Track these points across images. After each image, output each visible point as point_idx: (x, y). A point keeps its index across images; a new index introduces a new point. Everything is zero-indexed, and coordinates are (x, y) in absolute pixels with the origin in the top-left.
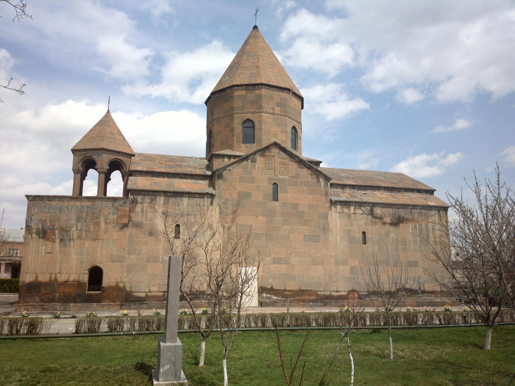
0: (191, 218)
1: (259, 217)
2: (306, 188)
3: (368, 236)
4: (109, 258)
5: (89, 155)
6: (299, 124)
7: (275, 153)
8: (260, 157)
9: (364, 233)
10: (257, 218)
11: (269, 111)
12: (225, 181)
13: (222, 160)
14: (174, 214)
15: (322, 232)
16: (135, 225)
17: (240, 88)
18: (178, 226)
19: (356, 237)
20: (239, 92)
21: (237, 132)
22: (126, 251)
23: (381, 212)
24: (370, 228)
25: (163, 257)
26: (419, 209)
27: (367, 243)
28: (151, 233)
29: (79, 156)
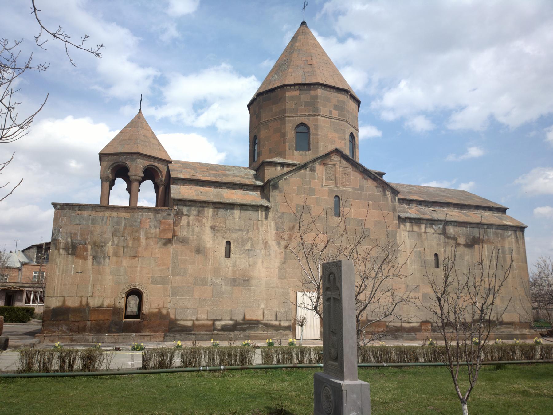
0: (243, 233)
3: (441, 258)
4: (150, 279)
5: (120, 160)
7: (337, 161)
9: (436, 255)
11: (326, 115)
12: (280, 192)
13: (274, 169)
14: (224, 229)
16: (181, 240)
17: (292, 87)
18: (228, 243)
19: (427, 259)
20: (291, 92)
22: (170, 272)
23: (454, 231)
25: (212, 279)
26: (495, 229)
28: (199, 251)
29: (108, 161)
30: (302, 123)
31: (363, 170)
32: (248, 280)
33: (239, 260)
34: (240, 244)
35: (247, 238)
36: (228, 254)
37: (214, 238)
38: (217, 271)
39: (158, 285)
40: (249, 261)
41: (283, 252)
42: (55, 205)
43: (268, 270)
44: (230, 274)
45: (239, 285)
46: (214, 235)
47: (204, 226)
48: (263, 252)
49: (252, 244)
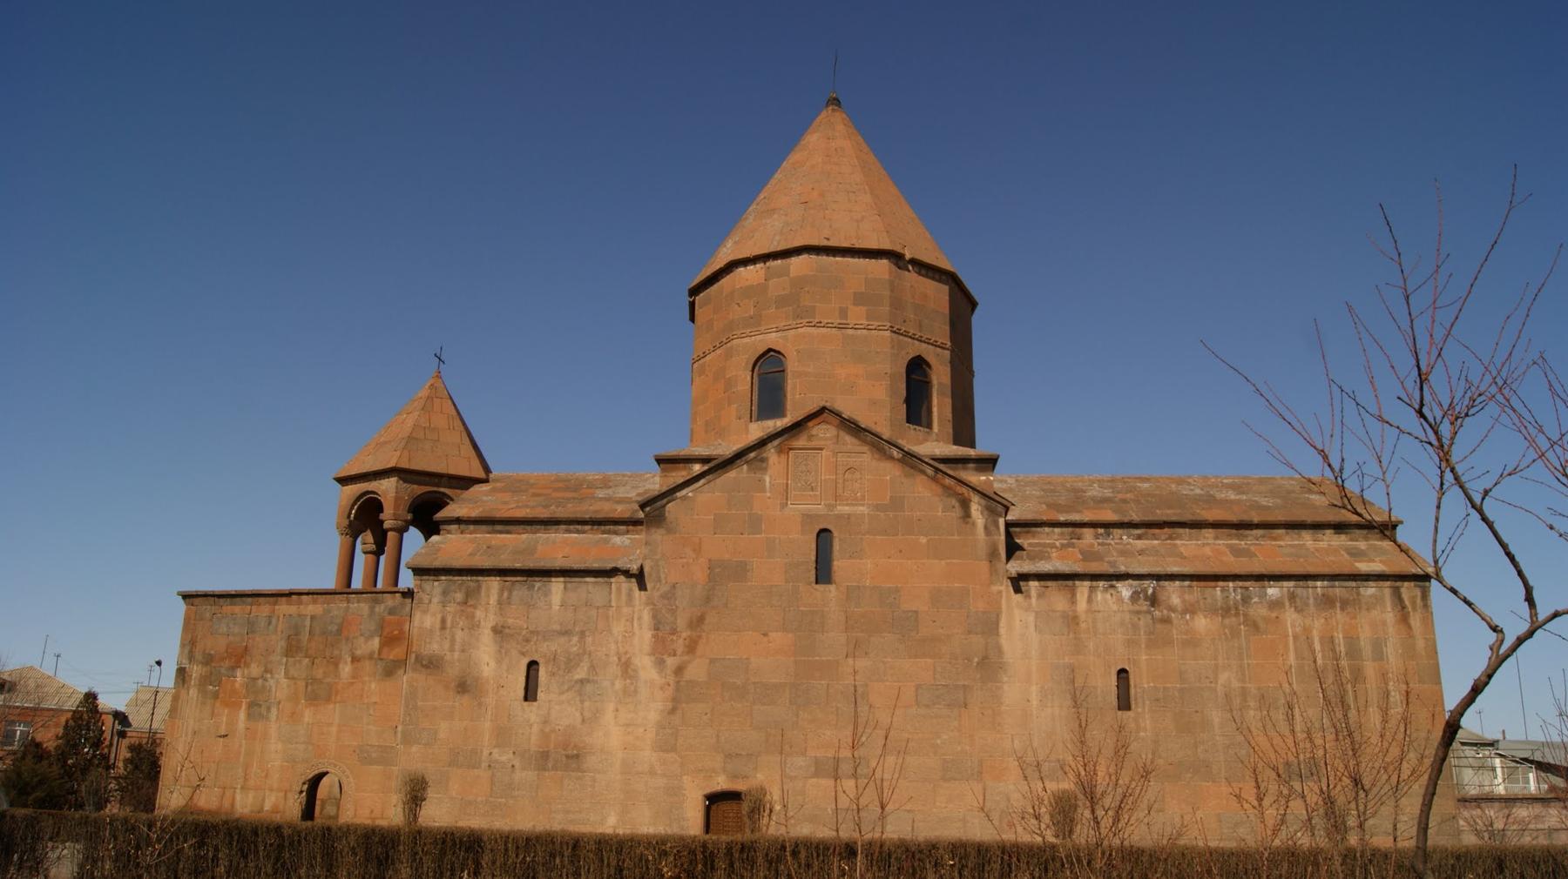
0: (570, 641)
1: (773, 635)
2: (923, 540)
3: (1140, 683)
4: (358, 751)
6: (939, 350)
7: (826, 439)
8: (779, 456)
9: (1122, 673)
10: (766, 639)
11: (829, 321)
12: (670, 531)
14: (524, 632)
15: (978, 676)
16: (424, 663)
18: (533, 665)
19: (1095, 688)
21: (739, 388)
22: (399, 735)
23: (1184, 601)
24: (1144, 658)
25: (491, 754)
27: (1133, 706)
28: (463, 686)
30: (770, 350)
31: (901, 455)
32: (577, 756)
33: (557, 707)
34: (563, 667)
35: (581, 651)
36: (530, 694)
37: (501, 654)
38: (502, 735)
39: (371, 764)
40: (583, 708)
41: (672, 682)
42: (187, 597)
43: (630, 729)
44: (534, 739)
45: (555, 768)
46: (501, 647)
47: (478, 626)
48: (618, 685)
49: (593, 667)
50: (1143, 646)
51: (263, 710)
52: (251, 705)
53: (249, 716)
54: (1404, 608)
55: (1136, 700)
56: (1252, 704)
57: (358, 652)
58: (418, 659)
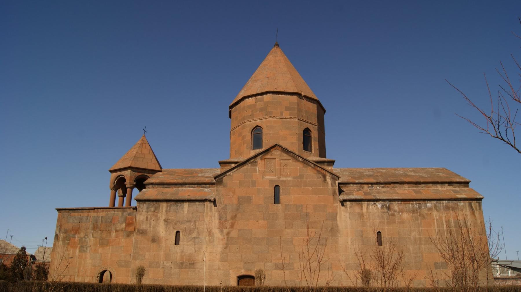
0: (190, 224)
1: (260, 221)
2: (311, 189)
3: (385, 236)
4: (117, 262)
6: (314, 126)
7: (277, 155)
8: (261, 161)
10: (257, 223)
12: (224, 186)
15: (330, 235)
16: (140, 232)
18: (178, 233)
21: (247, 139)
23: (399, 208)
24: (386, 227)
25: (163, 263)
27: (383, 244)
28: (154, 240)
30: (257, 126)
31: (302, 160)
32: (193, 264)
33: (186, 247)
34: (188, 233)
35: (194, 227)
36: (177, 242)
37: (167, 229)
38: (167, 257)
39: (122, 267)
40: (195, 247)
41: (225, 238)
42: (59, 210)
43: (211, 254)
44: (178, 258)
45: (186, 268)
46: (167, 226)
47: (159, 219)
48: (207, 239)
49: (198, 233)
50: (386, 223)
51: (85, 249)
52: (80, 247)
53: (80, 251)
54: (473, 210)
55: (384, 242)
56: (423, 243)
57: (118, 229)
58: (138, 231)
